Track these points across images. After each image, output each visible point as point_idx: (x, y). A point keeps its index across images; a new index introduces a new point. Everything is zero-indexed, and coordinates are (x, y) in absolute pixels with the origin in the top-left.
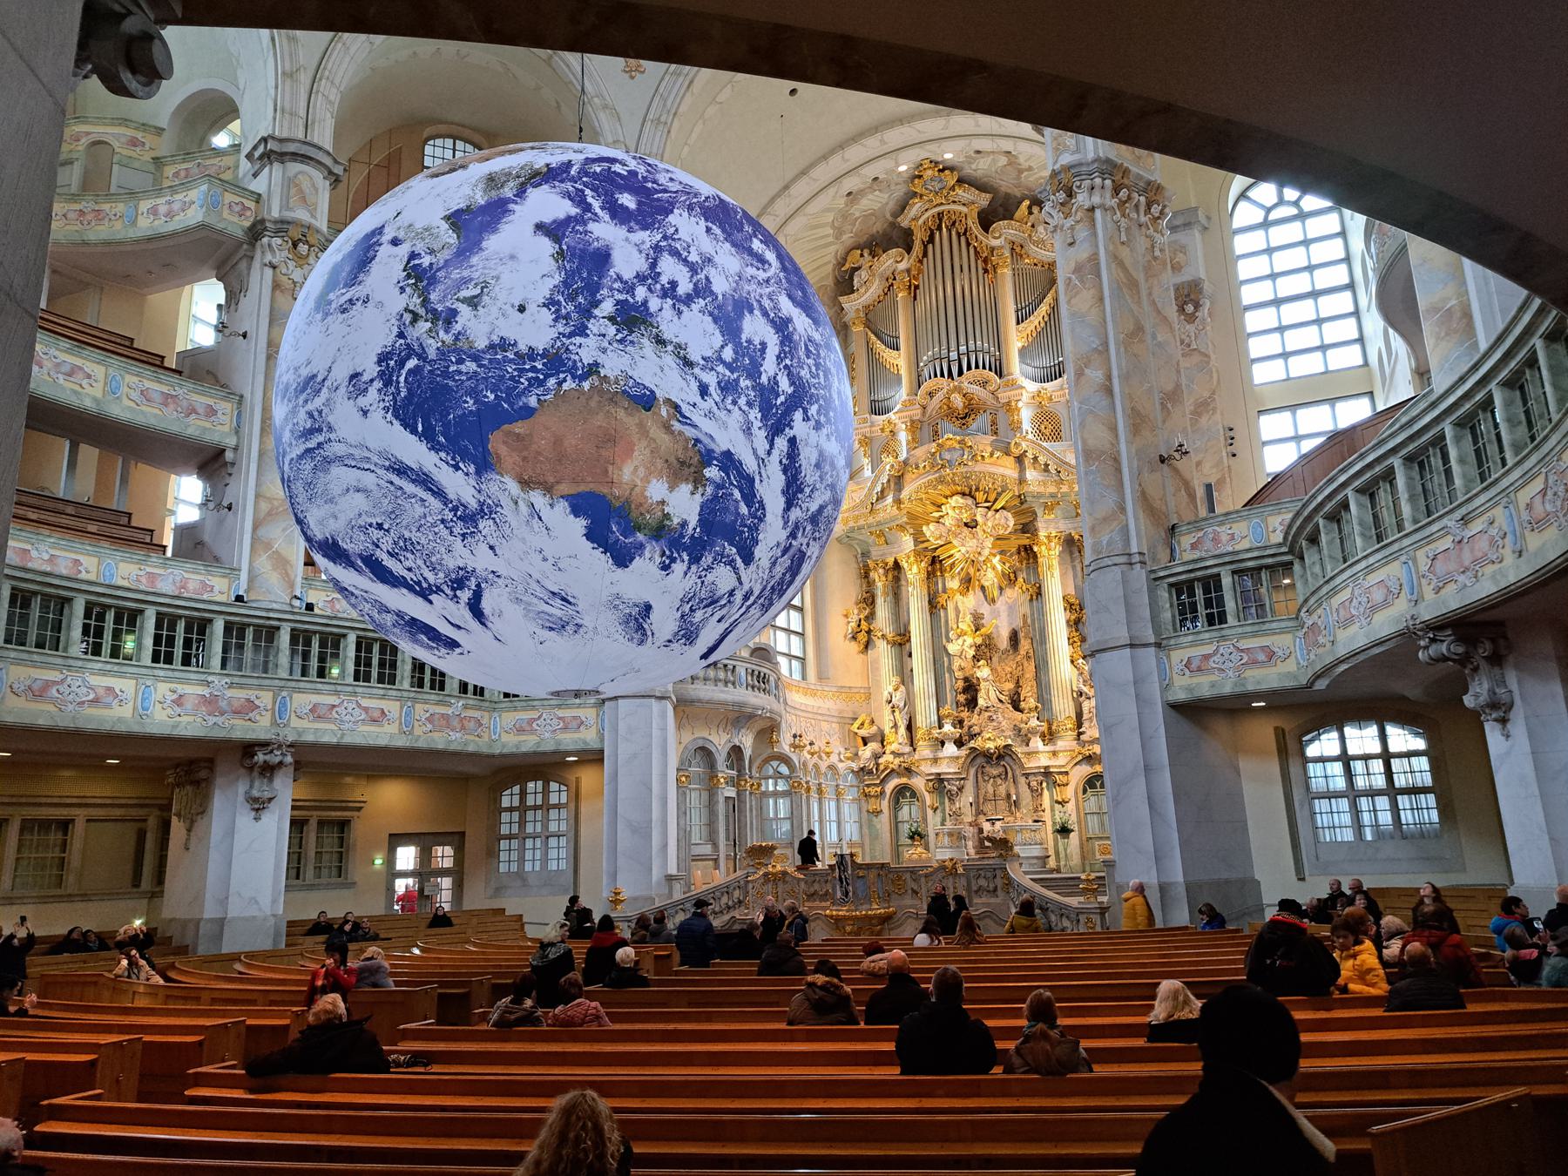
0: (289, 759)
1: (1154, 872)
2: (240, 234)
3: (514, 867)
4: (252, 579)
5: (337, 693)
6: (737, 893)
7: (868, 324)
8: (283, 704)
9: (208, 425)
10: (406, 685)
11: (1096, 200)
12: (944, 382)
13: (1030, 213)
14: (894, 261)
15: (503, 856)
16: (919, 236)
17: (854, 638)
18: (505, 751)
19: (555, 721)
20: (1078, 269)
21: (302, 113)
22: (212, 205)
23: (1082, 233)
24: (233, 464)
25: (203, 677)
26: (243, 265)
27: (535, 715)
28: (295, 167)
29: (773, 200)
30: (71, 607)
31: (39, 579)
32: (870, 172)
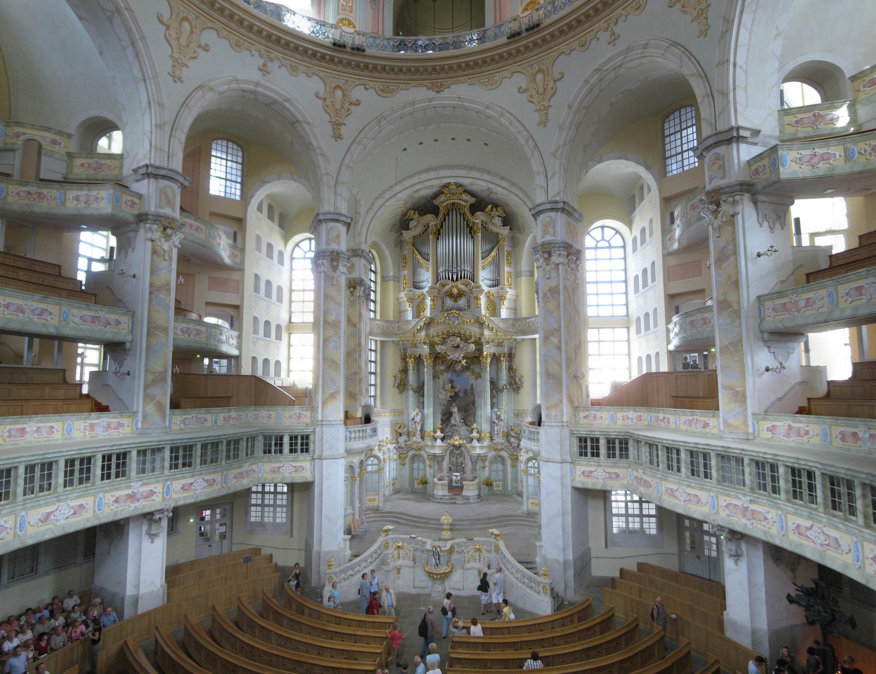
1: (562, 556)
2: (131, 218)
7: (414, 245)
11: (561, 260)
12: (450, 282)
13: (492, 210)
14: (429, 218)
16: (442, 212)
20: (550, 290)
21: (167, 150)
22: (116, 202)
23: (553, 274)
26: (132, 234)
28: (164, 183)
29: (384, 192)
32: (428, 184)
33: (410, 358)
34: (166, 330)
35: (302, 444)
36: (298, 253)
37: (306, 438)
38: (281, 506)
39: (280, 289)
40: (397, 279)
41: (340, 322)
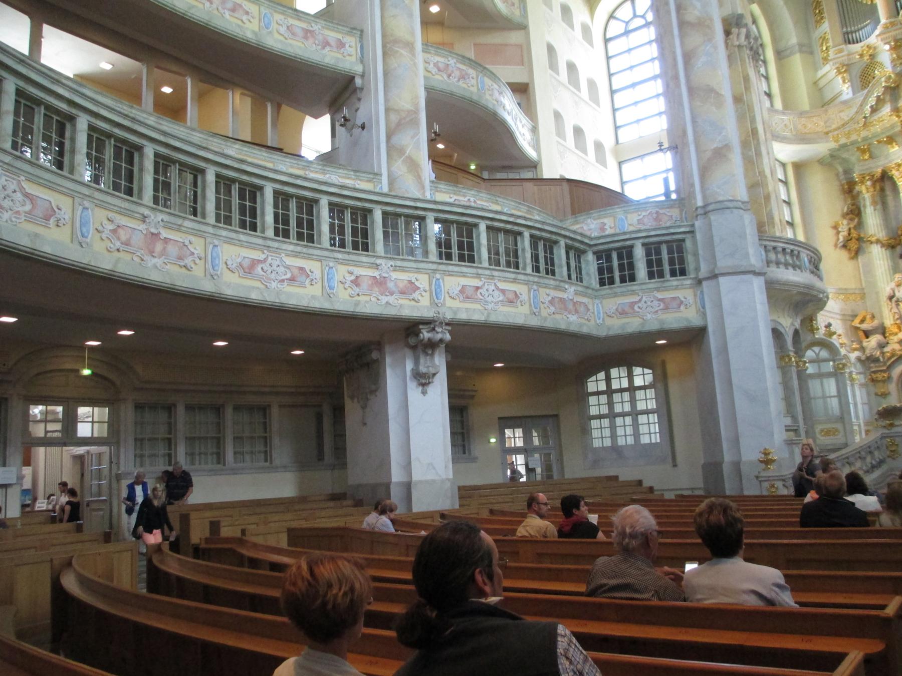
0: (448, 337)
3: (608, 443)
4: (391, 183)
5: (478, 276)
6: (876, 453)
8: (438, 286)
9: (340, 56)
10: (529, 270)
15: (595, 434)
17: (844, 246)
18: (611, 333)
19: (656, 303)
24: (362, 89)
25: (372, 260)
27: (637, 298)
30: (262, 195)
31: (236, 165)
33: (862, 182)
34: (410, 46)
35: (671, 262)
36: (616, 28)
37: (677, 247)
38: (647, 412)
39: (592, 84)
40: (807, 49)
41: (711, 20)
